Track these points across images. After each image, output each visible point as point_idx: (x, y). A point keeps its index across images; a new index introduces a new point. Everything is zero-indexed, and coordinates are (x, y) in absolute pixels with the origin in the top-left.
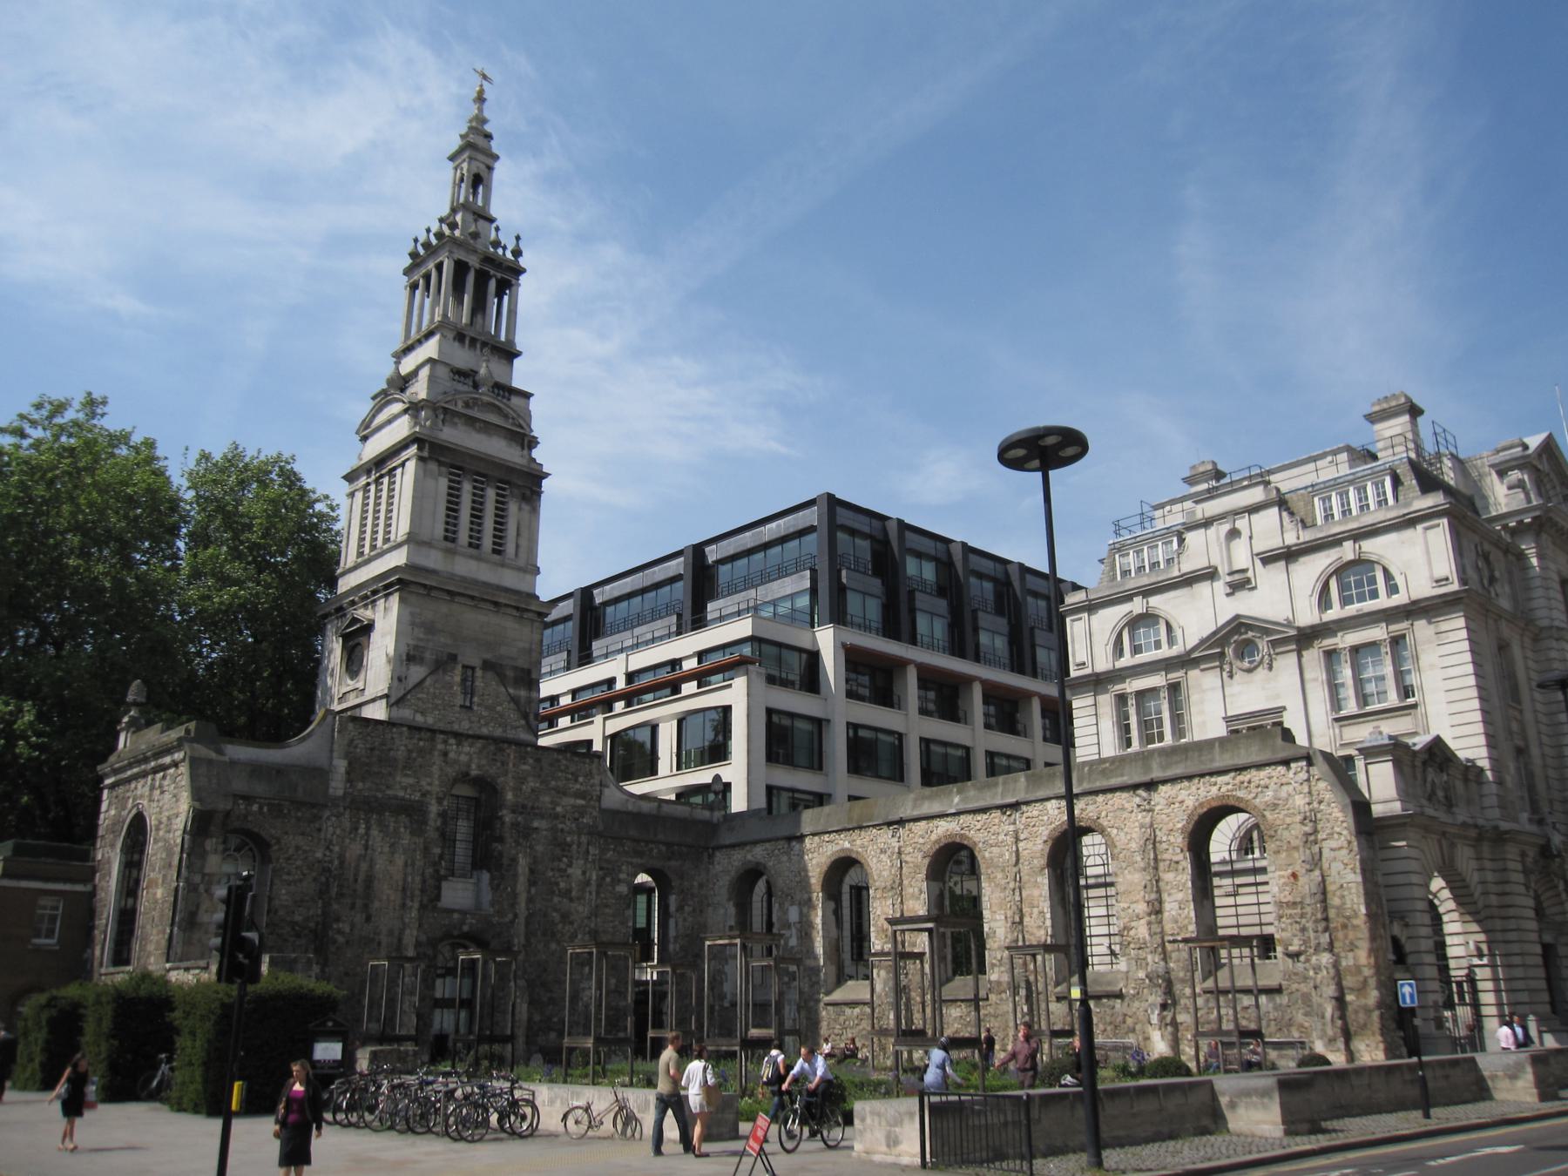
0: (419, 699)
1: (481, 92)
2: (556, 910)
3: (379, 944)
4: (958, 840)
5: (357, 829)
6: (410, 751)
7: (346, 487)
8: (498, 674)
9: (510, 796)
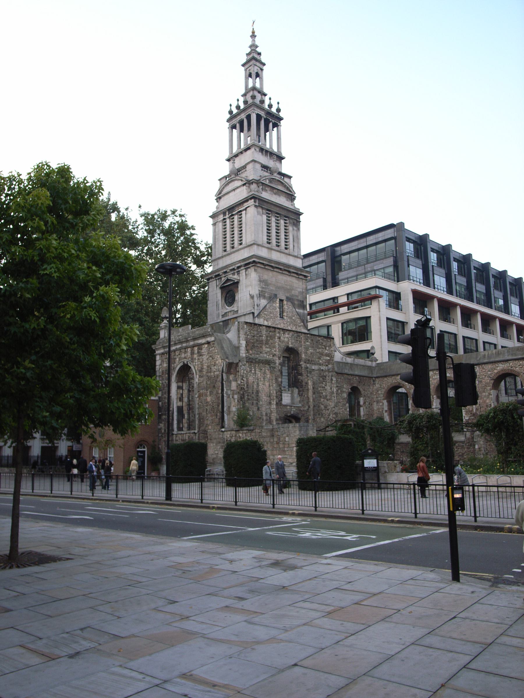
1: (253, 32)
2: (322, 404)
3: (263, 420)
5: (251, 371)
6: (267, 337)
7: (211, 221)
9: (303, 356)
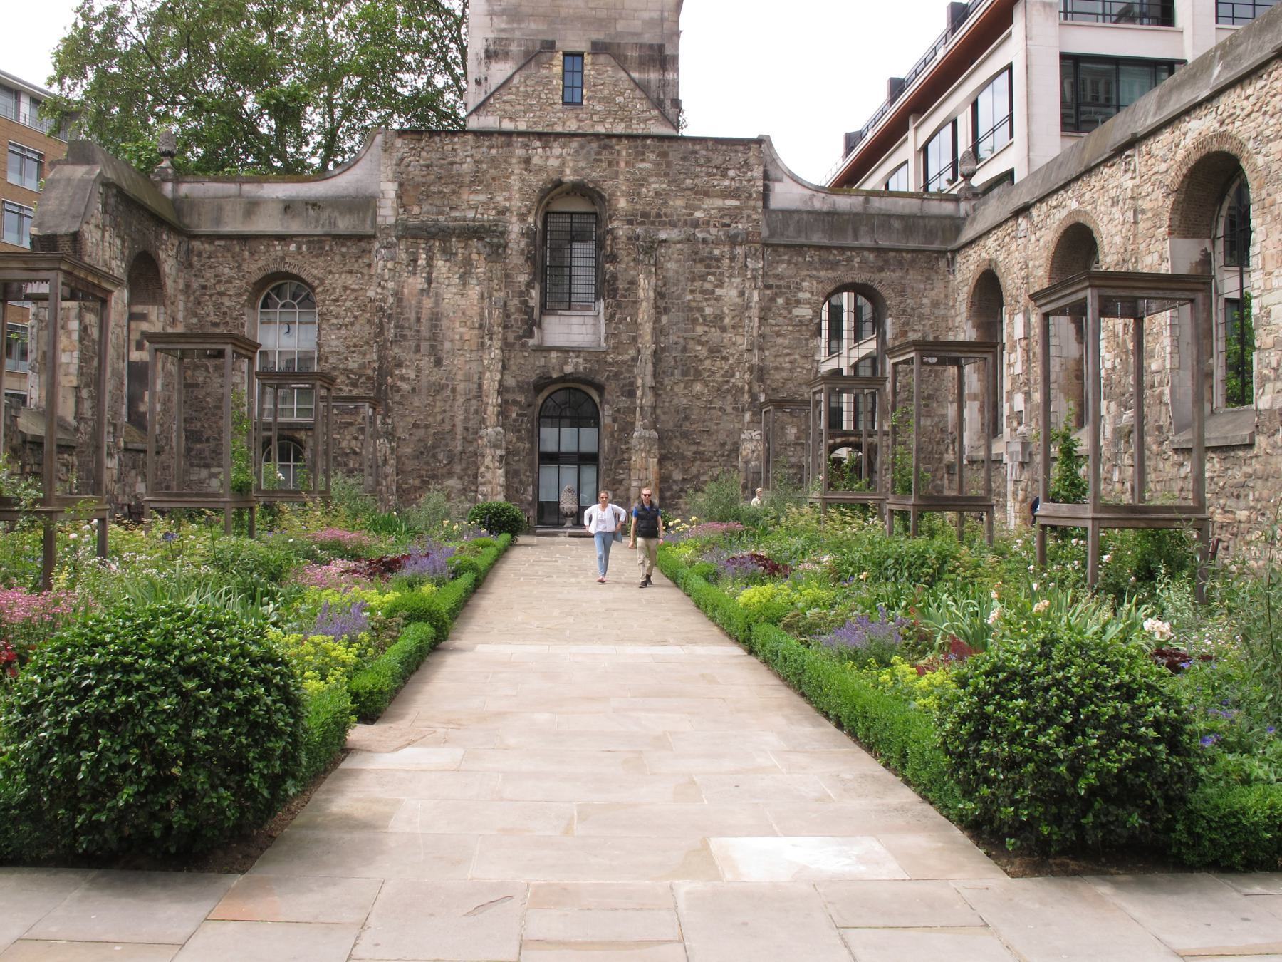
0: (505, 102)
2: (700, 343)
3: (454, 390)
4: (1215, 148)
5: (415, 261)
6: (478, 162)
8: (615, 57)
9: (622, 203)
